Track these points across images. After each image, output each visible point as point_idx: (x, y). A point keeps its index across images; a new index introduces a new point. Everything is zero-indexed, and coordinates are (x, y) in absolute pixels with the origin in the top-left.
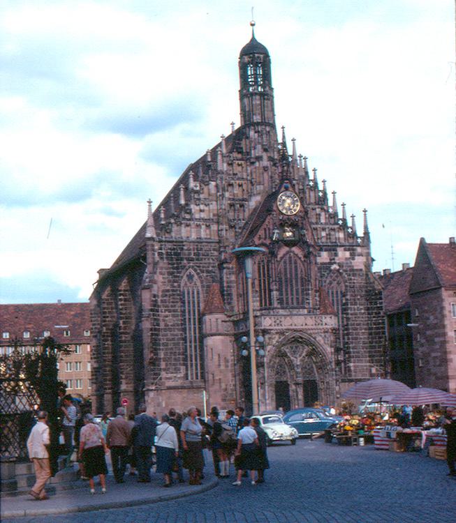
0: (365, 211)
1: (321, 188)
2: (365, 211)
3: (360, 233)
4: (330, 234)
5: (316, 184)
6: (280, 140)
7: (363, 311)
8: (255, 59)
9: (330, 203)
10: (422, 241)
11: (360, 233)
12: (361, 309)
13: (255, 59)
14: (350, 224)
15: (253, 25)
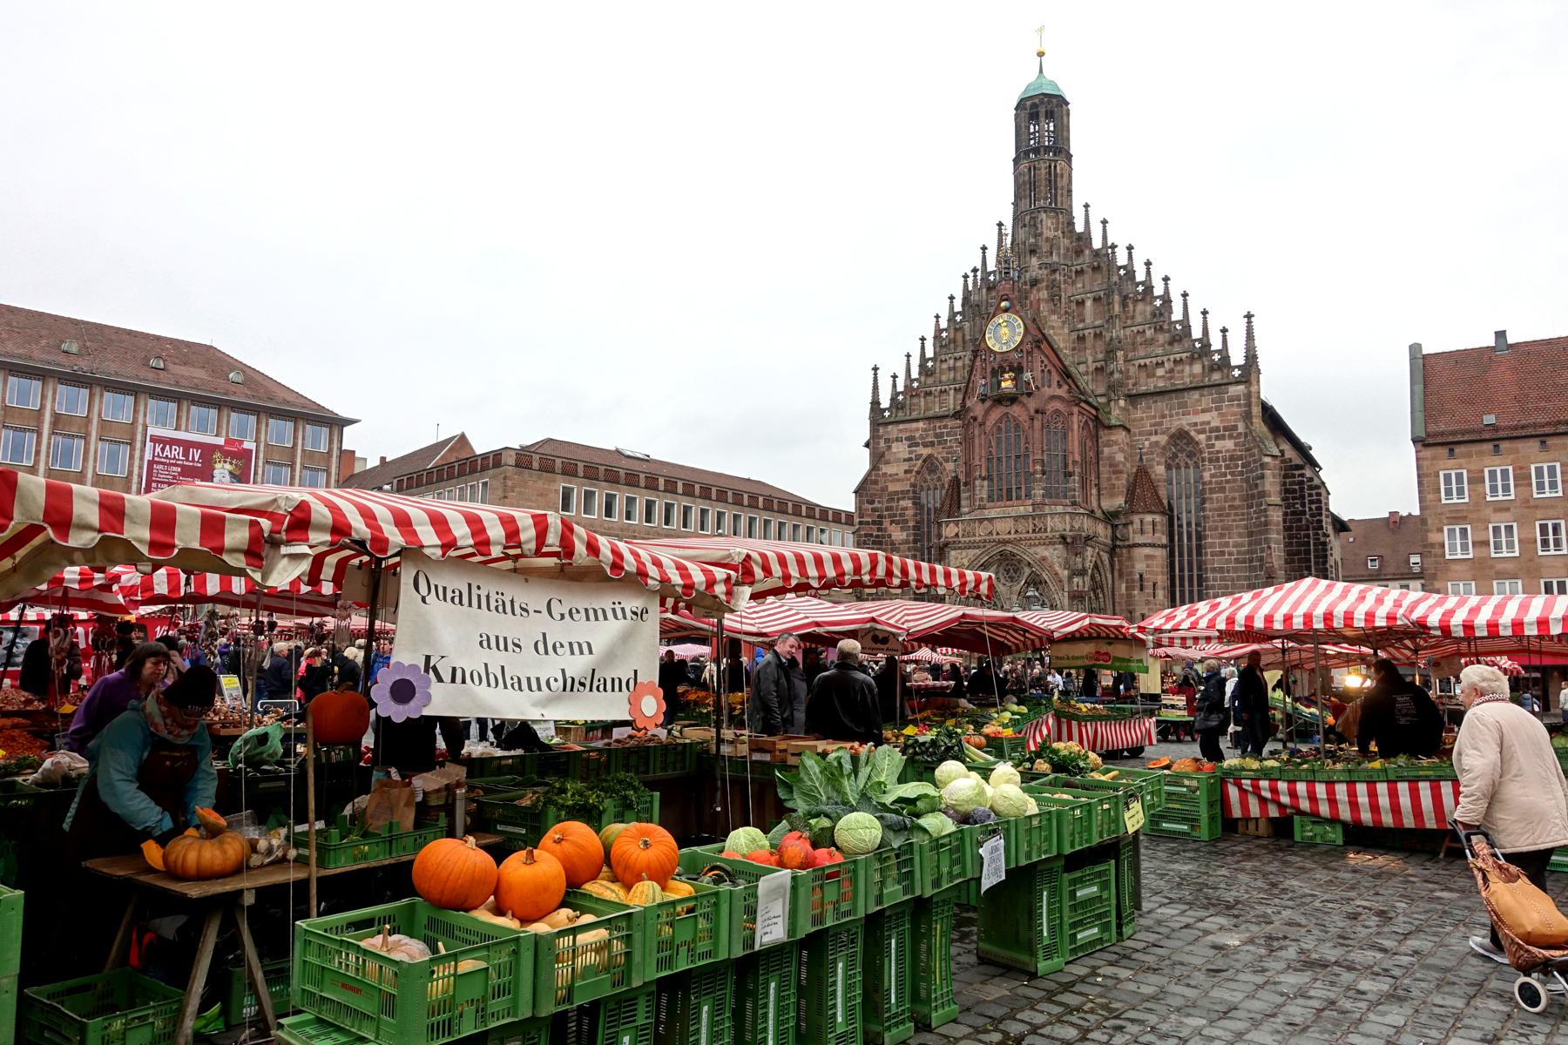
0: (1249, 316)
1: (1158, 290)
2: (1249, 316)
3: (1237, 357)
4: (1171, 371)
5: (1149, 288)
6: (1079, 228)
7: (1237, 503)
8: (1042, 115)
9: (1177, 315)
10: (1415, 349)
11: (1237, 357)
12: (1234, 499)
13: (1042, 115)
14: (1216, 344)
15: (1041, 54)
